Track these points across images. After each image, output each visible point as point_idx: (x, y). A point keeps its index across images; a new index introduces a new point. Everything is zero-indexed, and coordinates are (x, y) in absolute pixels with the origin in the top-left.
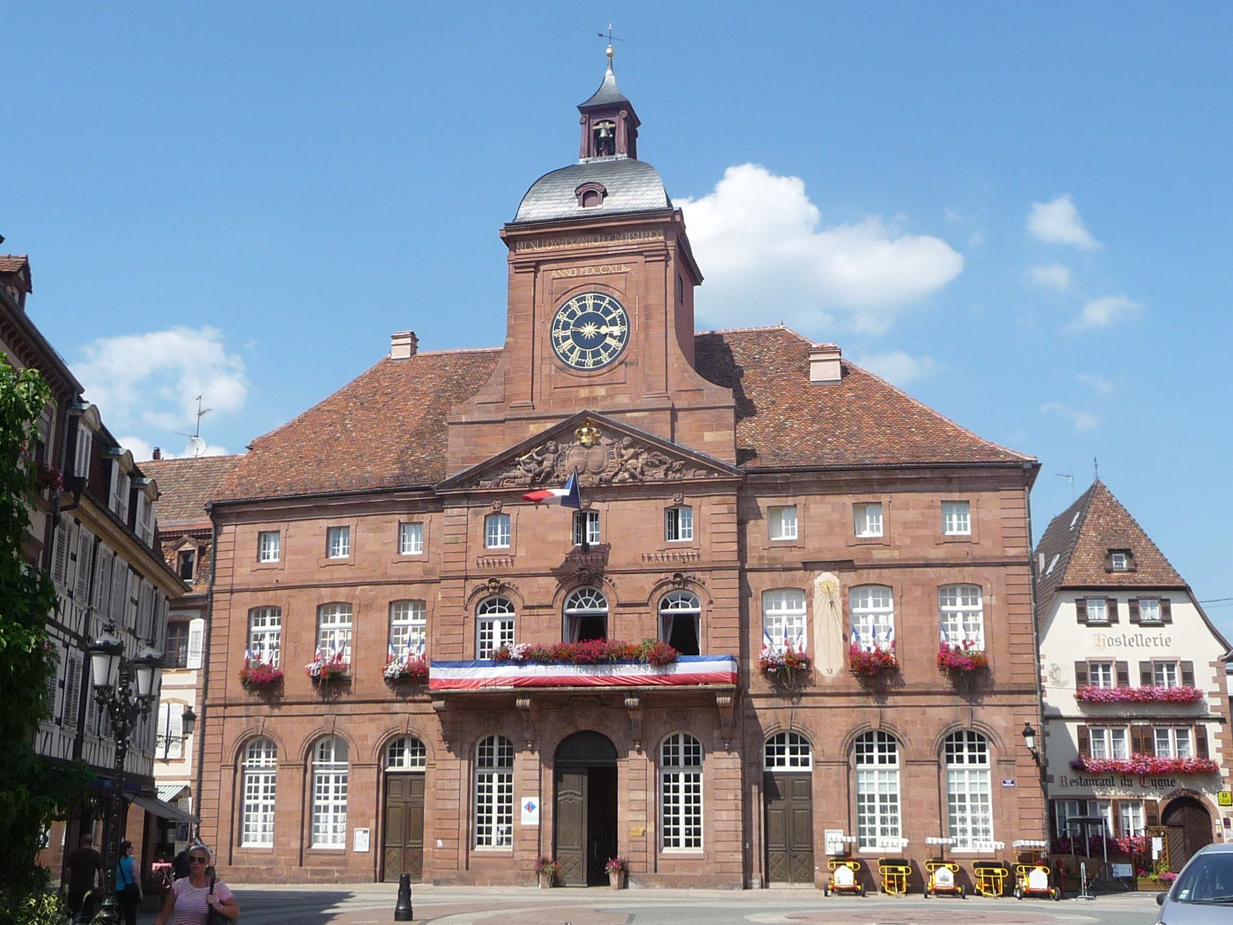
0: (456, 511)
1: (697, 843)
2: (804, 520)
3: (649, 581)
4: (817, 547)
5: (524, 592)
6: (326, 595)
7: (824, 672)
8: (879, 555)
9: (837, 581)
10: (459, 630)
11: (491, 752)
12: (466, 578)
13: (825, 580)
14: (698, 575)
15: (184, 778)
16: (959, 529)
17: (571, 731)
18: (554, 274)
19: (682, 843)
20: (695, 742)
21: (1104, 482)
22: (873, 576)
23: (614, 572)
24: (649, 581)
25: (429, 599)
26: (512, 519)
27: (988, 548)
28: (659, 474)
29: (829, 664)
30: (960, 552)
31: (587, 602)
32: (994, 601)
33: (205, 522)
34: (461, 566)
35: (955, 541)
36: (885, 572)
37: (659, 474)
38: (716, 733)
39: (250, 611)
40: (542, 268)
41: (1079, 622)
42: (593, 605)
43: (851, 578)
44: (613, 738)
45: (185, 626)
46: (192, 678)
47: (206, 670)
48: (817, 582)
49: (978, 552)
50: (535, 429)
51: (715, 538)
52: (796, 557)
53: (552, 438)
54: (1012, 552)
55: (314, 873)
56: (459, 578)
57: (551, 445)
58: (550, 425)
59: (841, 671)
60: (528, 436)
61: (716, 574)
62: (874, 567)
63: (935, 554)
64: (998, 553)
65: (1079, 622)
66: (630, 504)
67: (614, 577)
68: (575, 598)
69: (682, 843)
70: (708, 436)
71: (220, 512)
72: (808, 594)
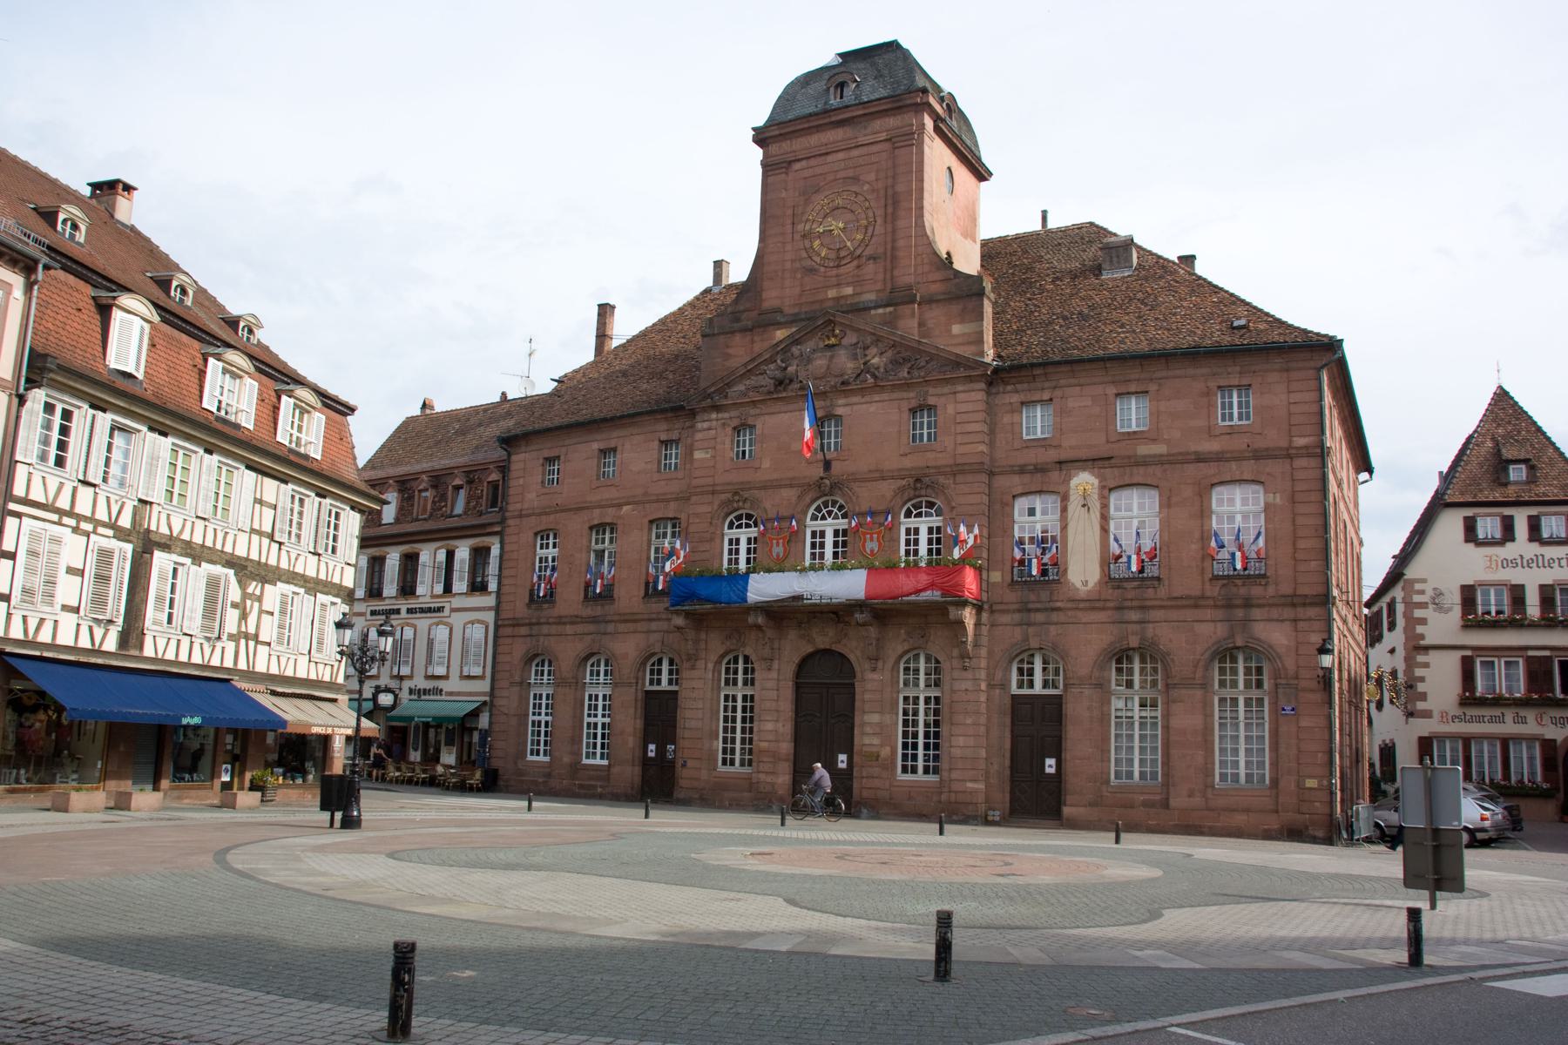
0: (705, 425)
1: (936, 771)
2: (1062, 413)
3: (887, 488)
4: (1072, 445)
5: (768, 505)
6: (596, 517)
7: (1078, 585)
8: (1144, 450)
9: (1096, 482)
10: (707, 546)
11: (736, 672)
12: (713, 493)
13: (1084, 481)
14: (941, 479)
15: (483, 694)
16: (1240, 418)
17: (810, 649)
18: (806, 173)
19: (920, 770)
20: (937, 662)
21: (1507, 388)
22: (1139, 474)
23: (855, 480)
24: (887, 488)
25: (683, 516)
26: (758, 430)
27: (1273, 438)
29: (1083, 572)
30: (1239, 444)
31: (830, 513)
32: (1278, 500)
33: (500, 453)
34: (709, 481)
35: (1232, 432)
36: (1151, 469)
38: (956, 652)
39: (536, 534)
40: (797, 166)
41: (1467, 541)
42: (836, 517)
43: (1113, 476)
44: (852, 657)
45: (488, 549)
46: (490, 601)
47: (498, 593)
48: (1074, 482)
49: (1260, 443)
50: (780, 334)
51: (960, 439)
52: (1053, 455)
53: (797, 342)
54: (1300, 442)
55: (581, 786)
56: (707, 493)
57: (795, 350)
59: (1100, 582)
61: (960, 478)
62: (1137, 464)
63: (1213, 446)
64: (1284, 444)
65: (1467, 541)
66: (873, 408)
67: (855, 486)
68: (818, 509)
69: (920, 770)
70: (956, 329)
71: (509, 442)
72: (1065, 498)
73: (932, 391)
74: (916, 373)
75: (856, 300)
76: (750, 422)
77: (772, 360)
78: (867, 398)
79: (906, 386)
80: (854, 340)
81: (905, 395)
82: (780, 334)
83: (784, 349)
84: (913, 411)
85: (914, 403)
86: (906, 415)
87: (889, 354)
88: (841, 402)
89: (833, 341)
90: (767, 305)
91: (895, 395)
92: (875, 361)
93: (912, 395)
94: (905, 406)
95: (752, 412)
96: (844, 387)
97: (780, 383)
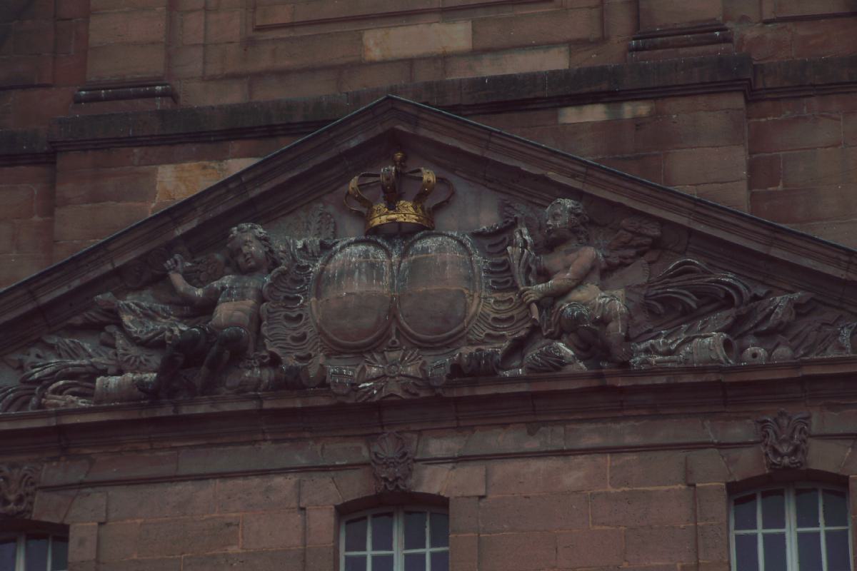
28: (708, 342)
37: (708, 342)
50: (175, 181)
57: (249, 237)
58: (237, 165)
60: (151, 208)
66: (574, 474)
73: (822, 420)
74: (755, 350)
75: (488, 68)
76: (45, 509)
77: (149, 275)
78: (554, 438)
79: (719, 393)
80: (488, 219)
81: (709, 431)
82: (175, 181)
83: (203, 231)
84: (740, 494)
85: (748, 463)
86: (718, 507)
87: (637, 274)
88: (438, 446)
89: (407, 213)
90: (104, 69)
91: (665, 432)
92: (592, 296)
93: (738, 431)
94: (714, 472)
95: (53, 473)
96: (470, 398)
97: (198, 358)
